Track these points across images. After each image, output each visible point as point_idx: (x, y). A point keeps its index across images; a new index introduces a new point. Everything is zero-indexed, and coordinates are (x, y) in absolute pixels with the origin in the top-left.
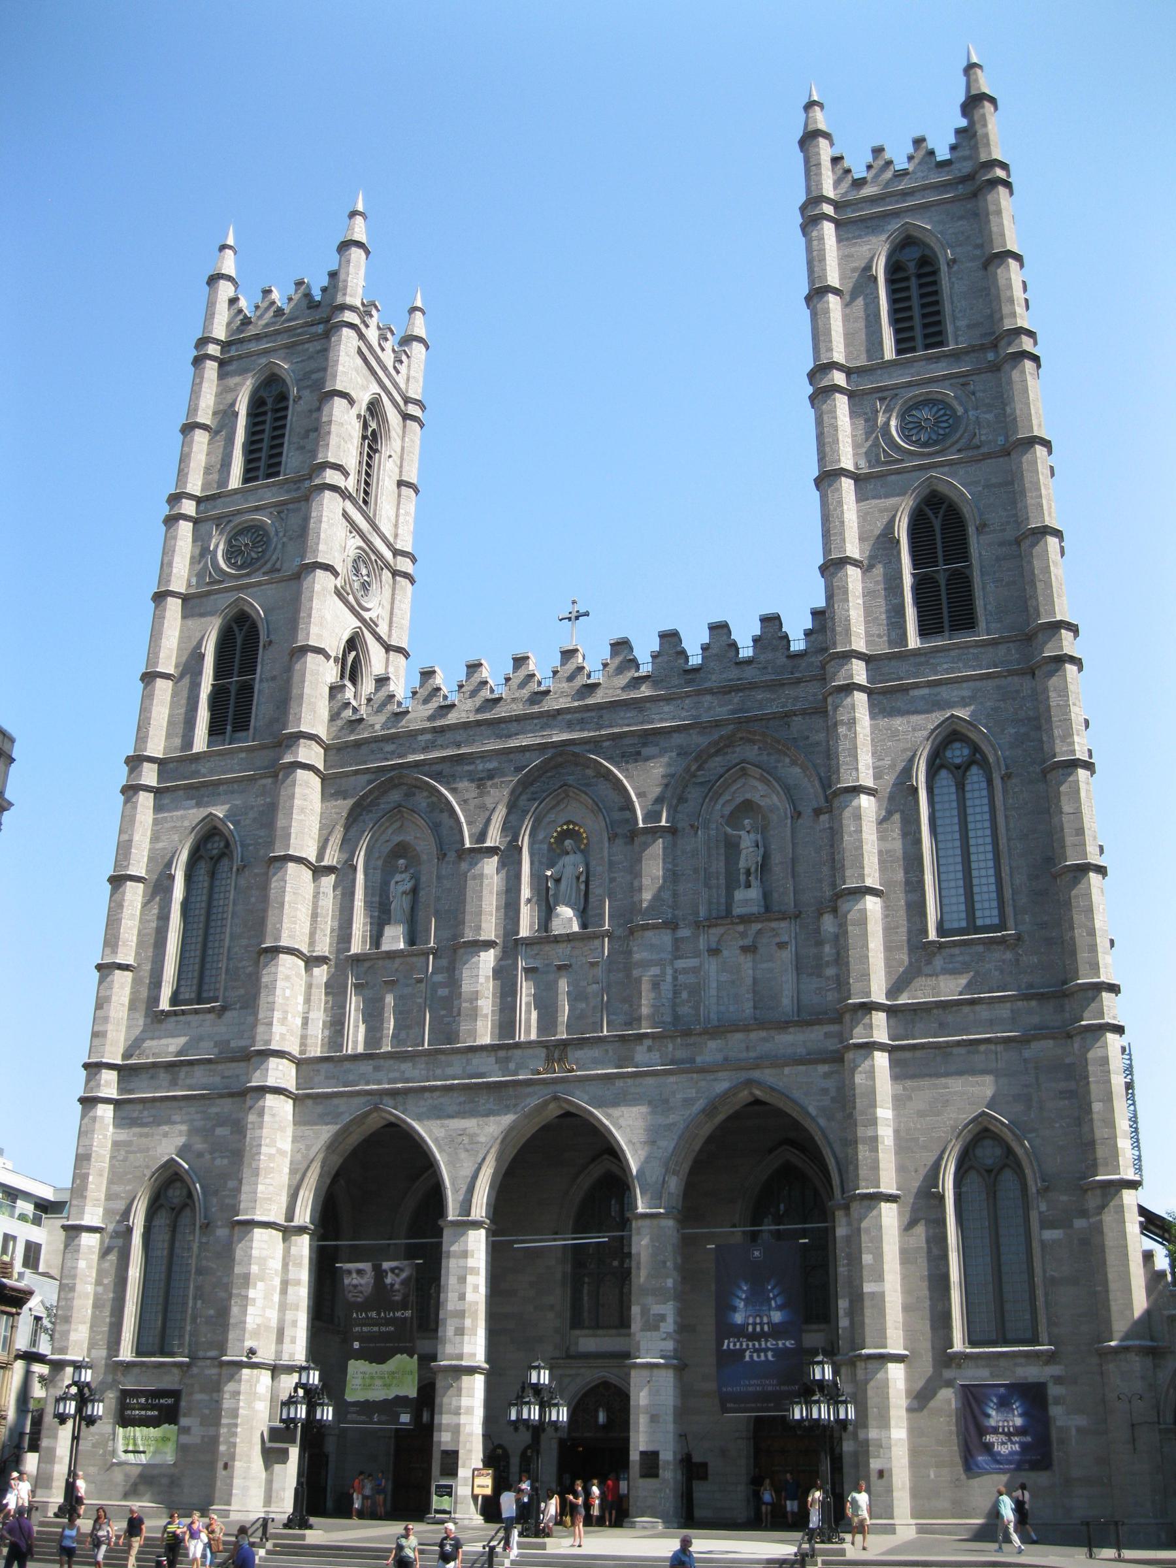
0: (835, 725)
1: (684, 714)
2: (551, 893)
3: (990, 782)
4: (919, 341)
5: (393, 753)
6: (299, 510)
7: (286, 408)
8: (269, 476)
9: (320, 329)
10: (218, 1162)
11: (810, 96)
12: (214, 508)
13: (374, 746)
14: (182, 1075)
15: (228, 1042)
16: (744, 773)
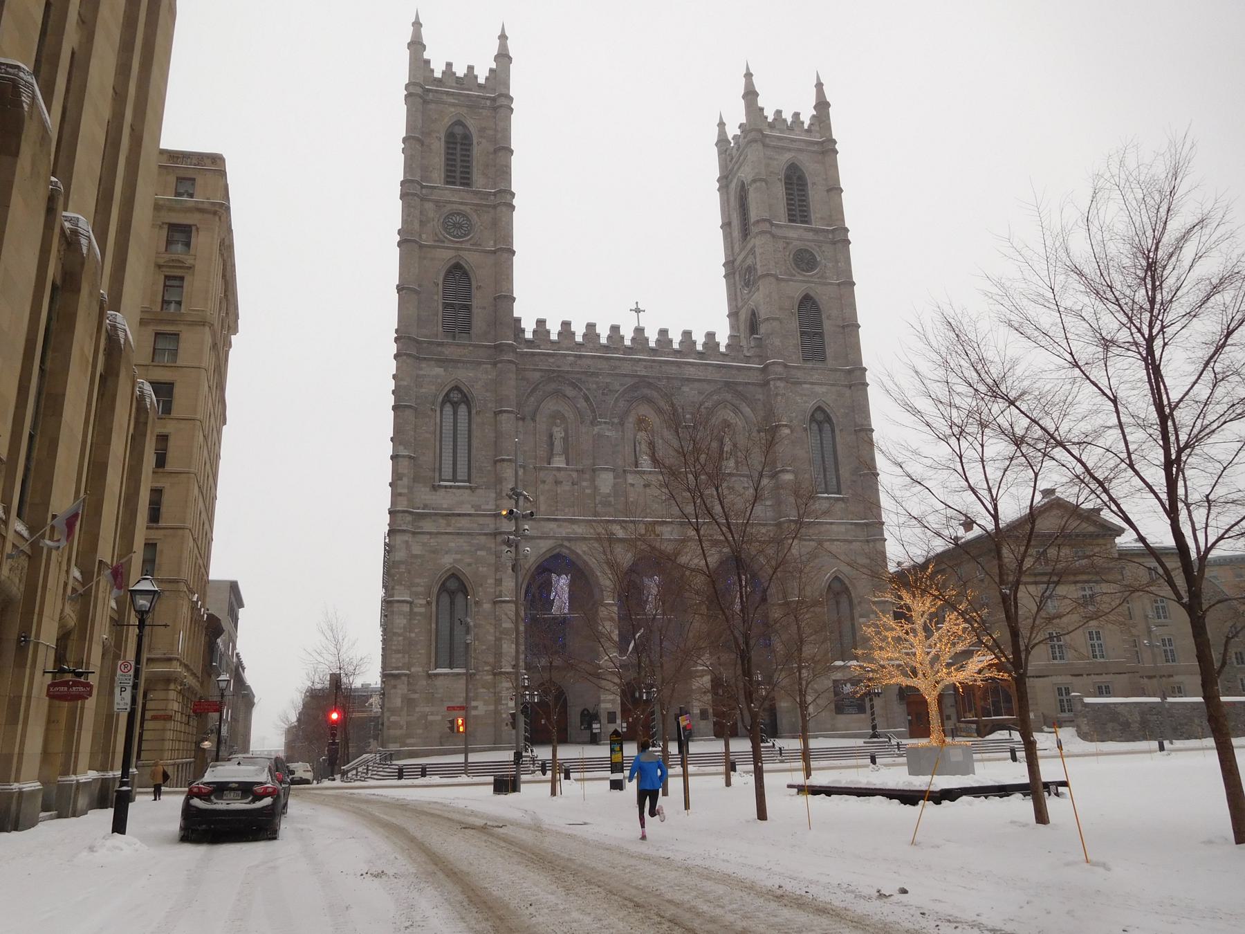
0: (777, 395)
1: (700, 374)
2: (638, 449)
3: (833, 431)
4: (799, 219)
5: (553, 363)
6: (489, 212)
7: (471, 144)
8: (462, 184)
9: (488, 103)
10: (481, 569)
11: (748, 68)
12: (432, 194)
13: (542, 357)
14: (453, 522)
15: (480, 506)
16: (725, 407)
